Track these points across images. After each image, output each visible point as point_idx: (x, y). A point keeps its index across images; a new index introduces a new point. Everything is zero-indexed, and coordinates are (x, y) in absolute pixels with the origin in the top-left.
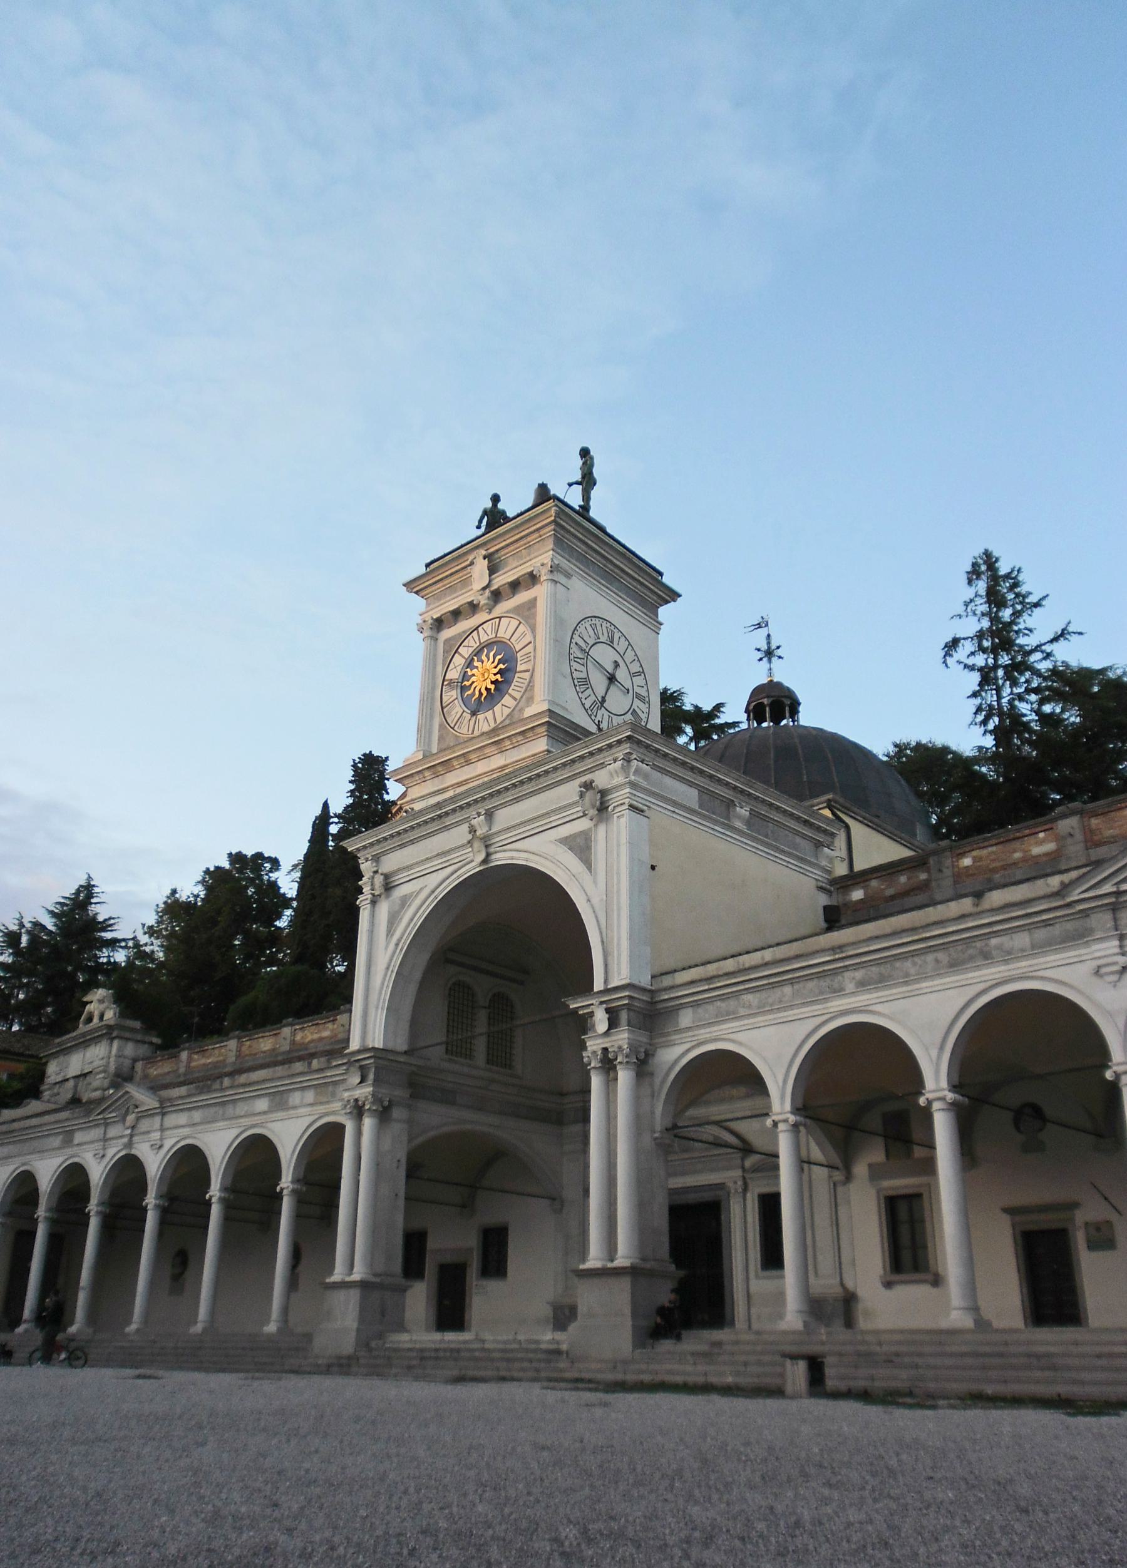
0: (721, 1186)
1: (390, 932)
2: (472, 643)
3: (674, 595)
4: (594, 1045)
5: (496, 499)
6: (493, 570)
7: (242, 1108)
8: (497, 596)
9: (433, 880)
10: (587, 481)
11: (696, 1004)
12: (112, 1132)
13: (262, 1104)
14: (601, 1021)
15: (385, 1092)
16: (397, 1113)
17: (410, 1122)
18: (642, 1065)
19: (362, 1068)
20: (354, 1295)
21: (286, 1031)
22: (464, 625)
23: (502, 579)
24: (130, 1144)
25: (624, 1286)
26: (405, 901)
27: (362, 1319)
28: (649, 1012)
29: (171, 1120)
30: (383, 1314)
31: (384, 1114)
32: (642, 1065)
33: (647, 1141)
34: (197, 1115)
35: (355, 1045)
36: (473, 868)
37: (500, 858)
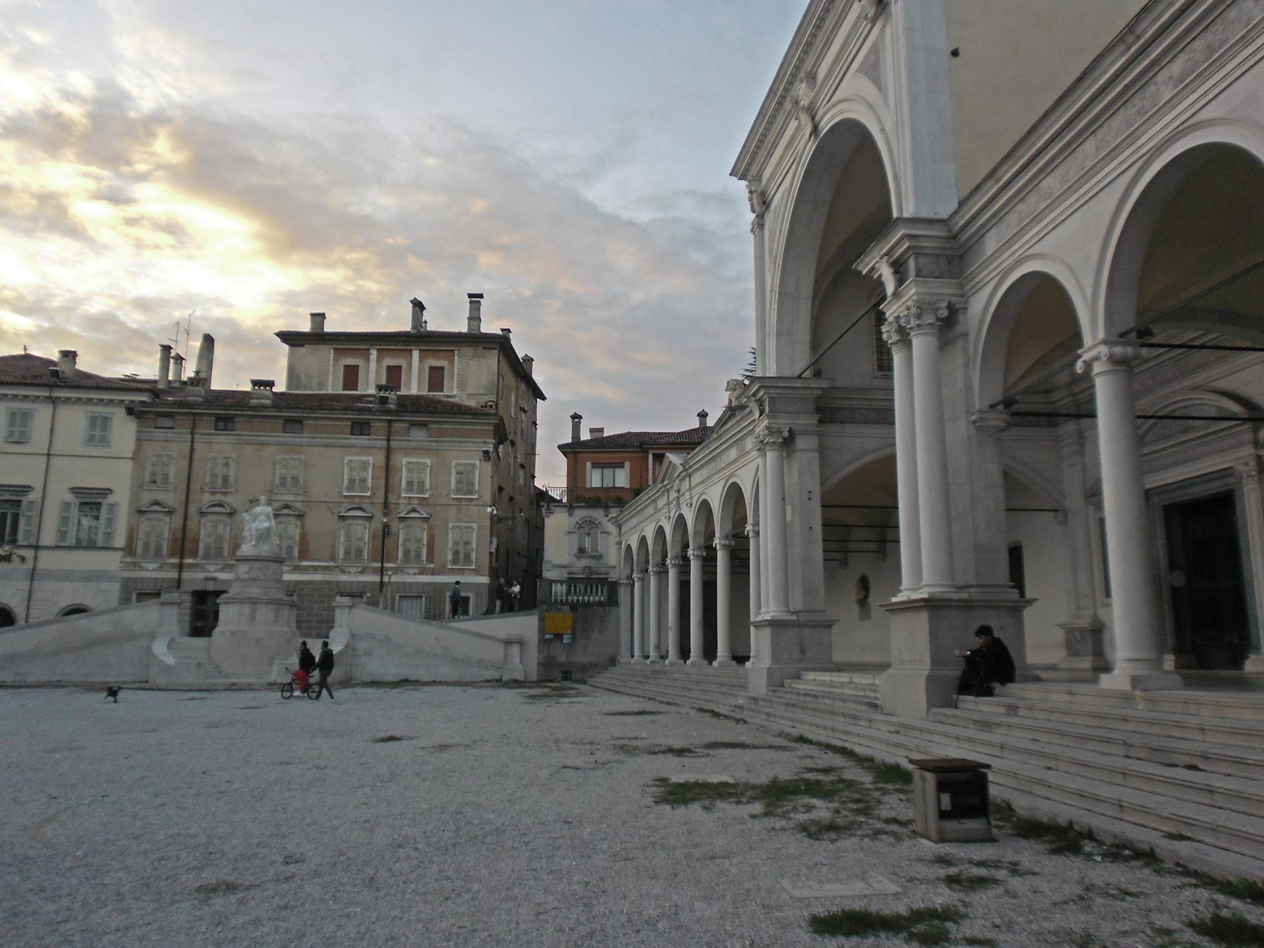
0: (1227, 472)
4: (892, 311)
11: (997, 218)
13: (733, 454)
15: (784, 423)
16: (801, 442)
17: (822, 450)
18: (948, 324)
19: (760, 403)
20: (767, 633)
24: (678, 506)
25: (922, 620)
27: (775, 657)
28: (953, 251)
29: (696, 478)
30: (803, 652)
31: (787, 443)
32: (948, 324)
33: (960, 430)
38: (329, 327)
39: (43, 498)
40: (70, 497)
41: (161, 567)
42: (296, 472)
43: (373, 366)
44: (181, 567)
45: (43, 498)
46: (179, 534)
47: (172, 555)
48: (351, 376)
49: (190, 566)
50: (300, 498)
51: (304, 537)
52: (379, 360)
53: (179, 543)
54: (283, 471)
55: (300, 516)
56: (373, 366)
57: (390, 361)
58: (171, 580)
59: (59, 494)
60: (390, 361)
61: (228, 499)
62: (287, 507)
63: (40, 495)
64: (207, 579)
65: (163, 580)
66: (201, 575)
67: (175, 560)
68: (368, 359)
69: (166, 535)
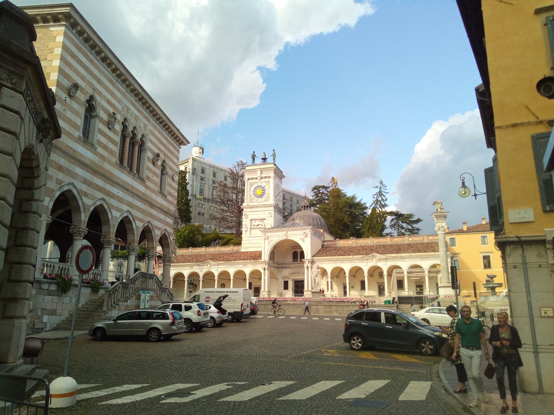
1: (268, 244)
2: (255, 186)
3: (284, 177)
5: (254, 152)
6: (261, 173)
7: (236, 266)
8: (262, 178)
9: (276, 239)
10: (274, 156)
12: (204, 267)
14: (307, 262)
21: (218, 248)
22: (253, 181)
23: (262, 176)
26: (271, 241)
34: (226, 266)
35: (263, 260)
36: (285, 238)
37: (288, 238)
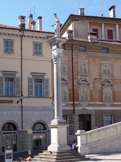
38: (86, 14)
39: (22, 76)
40: (31, 76)
41: (67, 105)
42: (108, 68)
43: (103, 29)
44: (74, 105)
45: (22, 76)
46: (72, 92)
47: (70, 101)
48: (95, 33)
49: (77, 104)
50: (110, 78)
51: (114, 92)
52: (105, 27)
53: (72, 95)
54: (104, 68)
55: (111, 85)
56: (103, 29)
57: (108, 28)
58: (71, 110)
59: (27, 76)
60: (108, 28)
61: (87, 78)
62: (108, 82)
63: (20, 75)
64: (83, 109)
65: (68, 110)
66: (81, 108)
67: (72, 103)
68: (101, 27)
69: (67, 92)
